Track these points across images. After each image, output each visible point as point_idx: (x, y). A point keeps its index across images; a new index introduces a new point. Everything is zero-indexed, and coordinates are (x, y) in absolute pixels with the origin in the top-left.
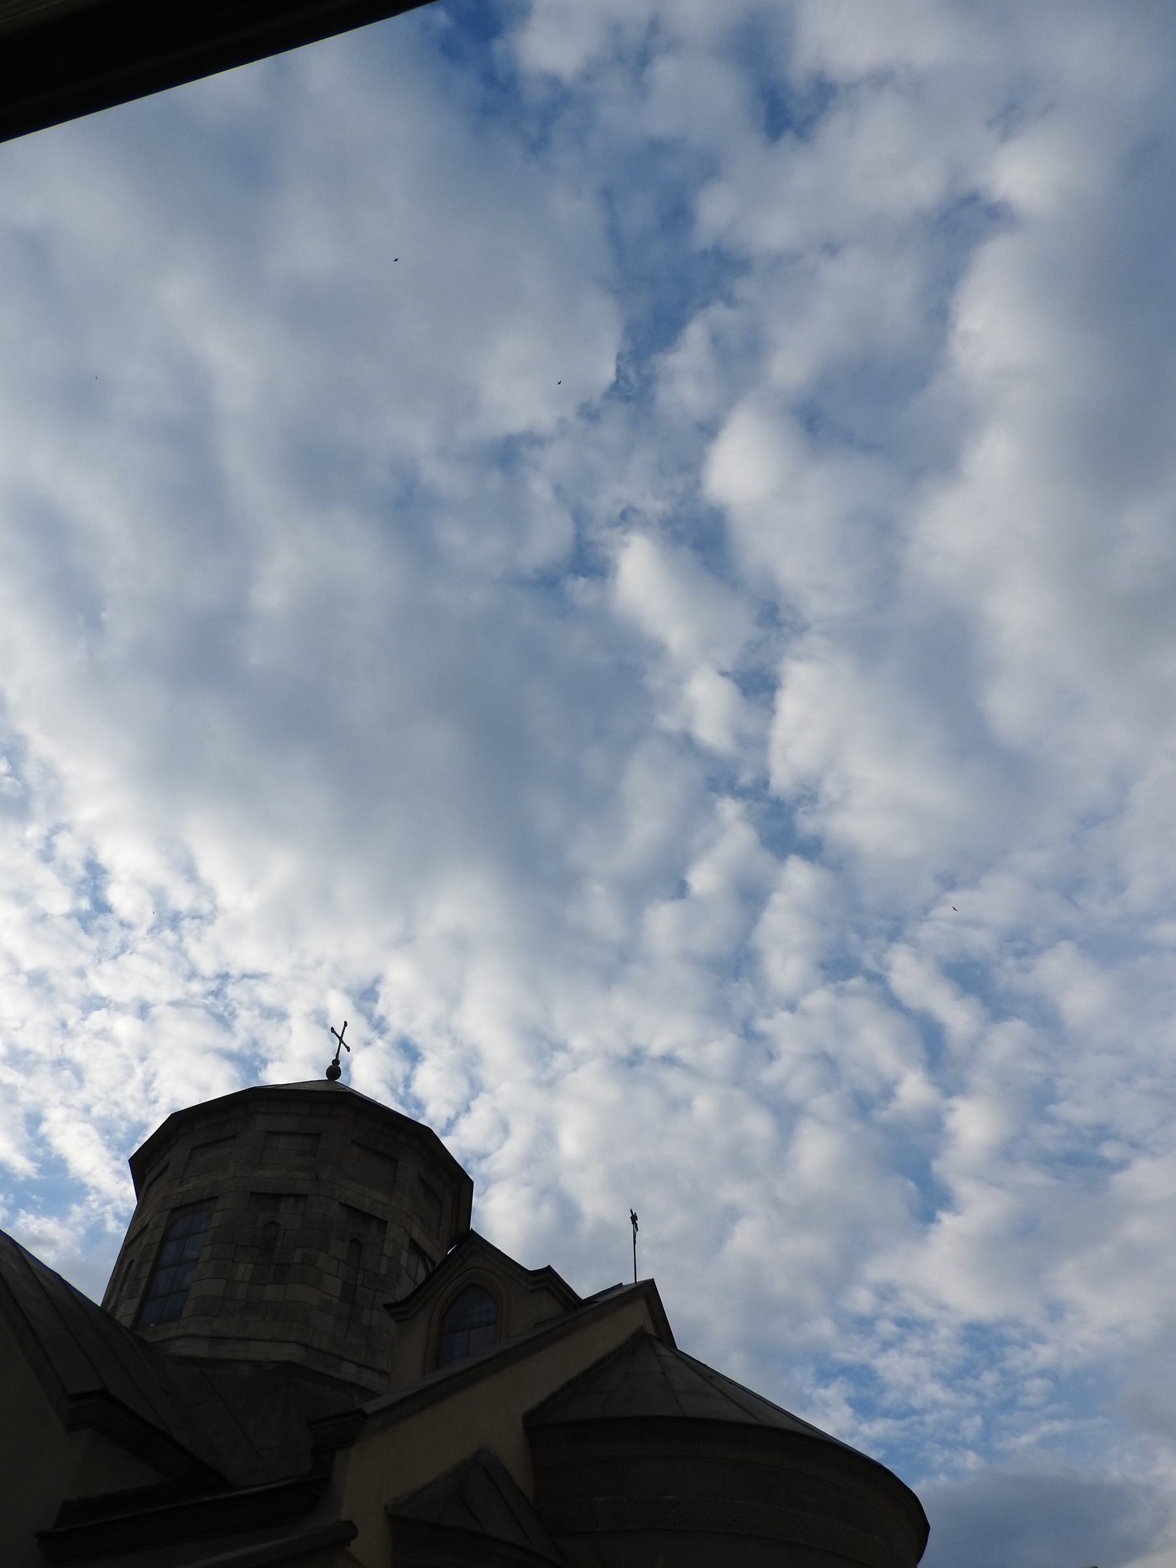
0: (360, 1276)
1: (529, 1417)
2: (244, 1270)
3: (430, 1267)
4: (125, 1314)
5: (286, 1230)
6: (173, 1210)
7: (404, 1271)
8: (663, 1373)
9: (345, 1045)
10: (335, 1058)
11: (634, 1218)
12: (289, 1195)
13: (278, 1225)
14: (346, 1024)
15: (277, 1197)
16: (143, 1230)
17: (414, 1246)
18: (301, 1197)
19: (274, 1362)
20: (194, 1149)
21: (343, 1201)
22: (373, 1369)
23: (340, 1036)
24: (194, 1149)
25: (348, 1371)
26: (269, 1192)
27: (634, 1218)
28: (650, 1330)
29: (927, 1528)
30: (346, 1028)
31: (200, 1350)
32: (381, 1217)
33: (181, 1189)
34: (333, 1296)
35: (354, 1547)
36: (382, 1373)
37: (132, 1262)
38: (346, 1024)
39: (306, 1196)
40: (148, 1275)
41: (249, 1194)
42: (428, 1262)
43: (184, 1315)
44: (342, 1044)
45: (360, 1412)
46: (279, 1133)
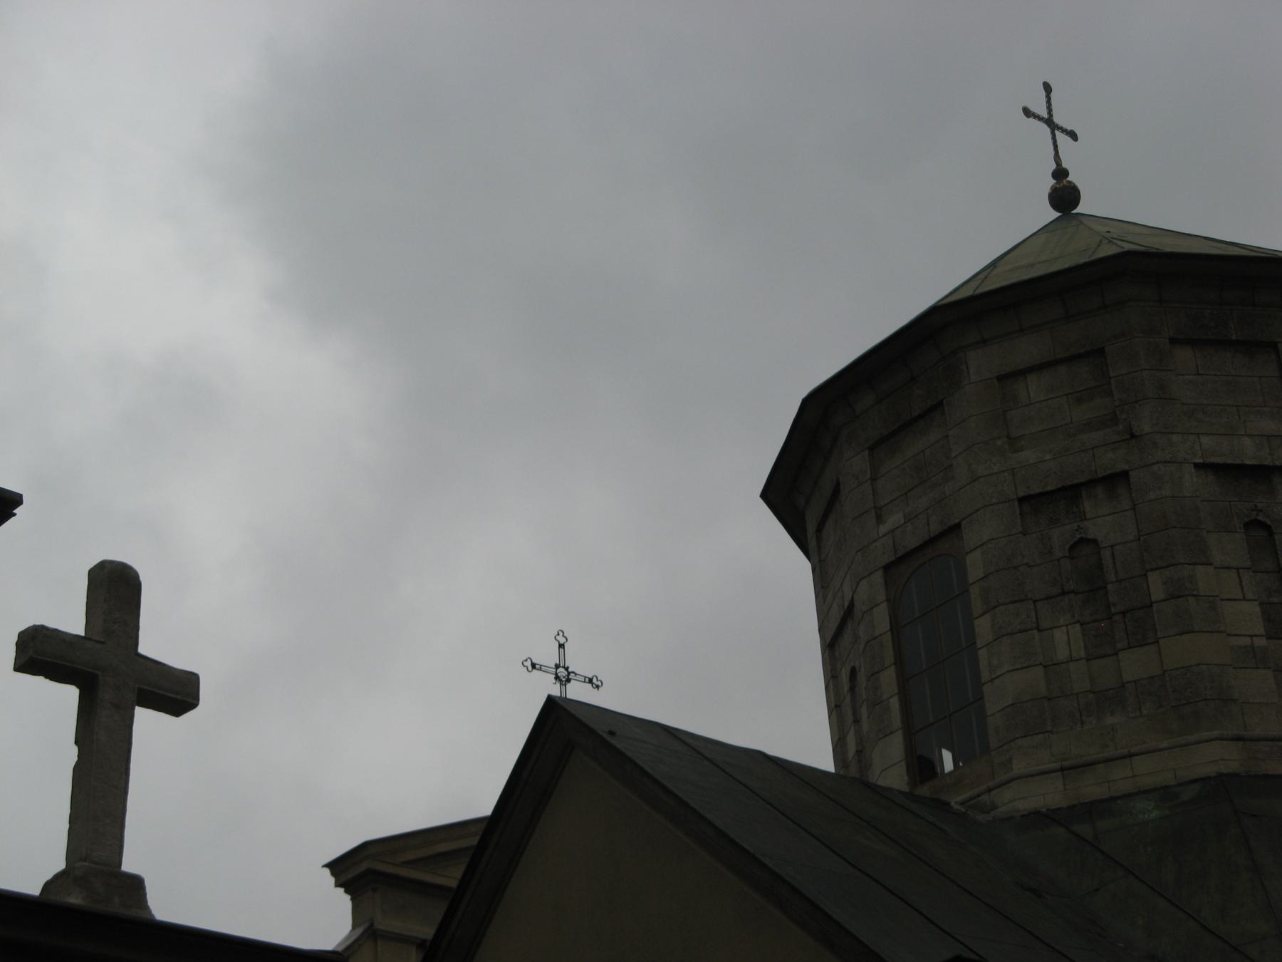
5: (1112, 547)
6: (887, 568)
9: (1064, 131)
10: (1054, 166)
12: (1092, 483)
13: (1094, 541)
14: (1047, 88)
16: (849, 613)
18: (1113, 481)
20: (871, 449)
23: (1046, 116)
26: (1049, 488)
30: (1053, 95)
31: (1050, 794)
33: (883, 529)
34: (1251, 636)
37: (853, 672)
38: (1047, 88)
39: (1125, 475)
40: (896, 690)
41: (1016, 503)
44: (1057, 132)
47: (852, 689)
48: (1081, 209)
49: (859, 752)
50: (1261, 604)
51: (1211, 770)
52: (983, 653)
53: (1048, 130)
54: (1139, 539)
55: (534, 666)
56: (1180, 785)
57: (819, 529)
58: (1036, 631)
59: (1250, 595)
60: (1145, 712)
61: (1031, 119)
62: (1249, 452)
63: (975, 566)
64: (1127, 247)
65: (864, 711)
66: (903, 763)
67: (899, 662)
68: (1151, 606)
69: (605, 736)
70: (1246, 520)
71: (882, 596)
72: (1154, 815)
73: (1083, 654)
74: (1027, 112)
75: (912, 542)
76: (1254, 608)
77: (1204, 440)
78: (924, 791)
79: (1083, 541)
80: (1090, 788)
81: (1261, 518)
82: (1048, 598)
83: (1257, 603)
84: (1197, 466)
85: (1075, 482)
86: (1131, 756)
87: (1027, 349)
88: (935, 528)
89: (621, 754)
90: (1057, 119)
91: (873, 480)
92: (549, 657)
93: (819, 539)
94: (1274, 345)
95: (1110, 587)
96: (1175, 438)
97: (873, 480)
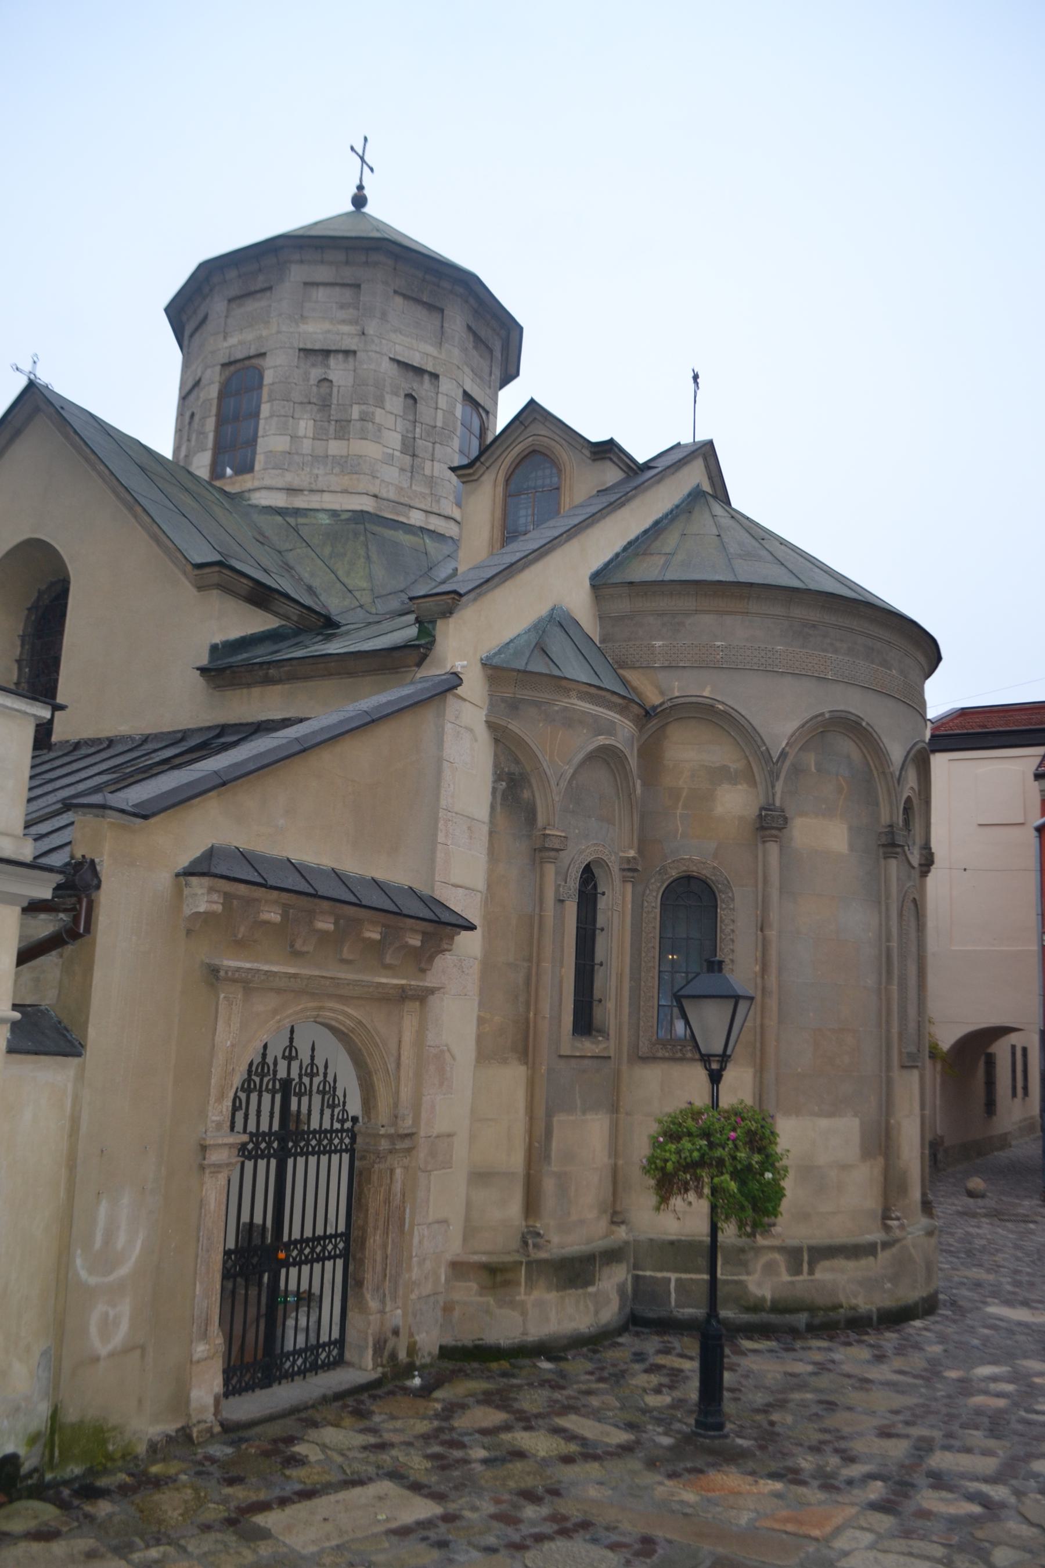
0: (418, 430)
1: (595, 576)
2: (305, 426)
3: (484, 415)
4: (201, 465)
5: (339, 386)
6: (224, 365)
7: (459, 423)
8: (719, 536)
10: (358, 182)
11: (696, 377)
12: (337, 351)
13: (331, 381)
14: (366, 139)
15: (327, 353)
16: (197, 384)
17: (467, 396)
18: (348, 353)
19: (350, 511)
20: (230, 301)
21: (392, 356)
22: (439, 515)
24: (230, 301)
25: (416, 518)
26: (317, 347)
27: (696, 377)
28: (707, 487)
29: (939, 659)
30: (368, 145)
31: (279, 500)
32: (433, 371)
33: (226, 344)
35: (460, 691)
37: (193, 415)
38: (366, 139)
39: (354, 352)
42: (481, 411)
43: (257, 467)
44: (365, 165)
45: (455, 592)
46: (316, 284)
47: (190, 423)
48: (366, 210)
49: (186, 456)
51: (358, 508)
52: (262, 422)
55: (17, 369)
56: (342, 511)
57: (191, 336)
58: (291, 419)
59: (398, 429)
62: (416, 361)
63: (269, 378)
64: (386, 236)
65: (194, 437)
66: (208, 468)
67: (218, 415)
68: (350, 421)
69: (60, 409)
70: (406, 392)
71: (217, 378)
73: (311, 435)
74: (352, 149)
75: (239, 355)
76: (399, 437)
77: (397, 346)
78: (217, 483)
79: (325, 380)
80: (300, 502)
81: (414, 394)
82: (301, 403)
84: (391, 359)
85: (330, 348)
86: (323, 491)
87: (324, 273)
88: (252, 352)
89: (65, 419)
90: (366, 158)
91: (227, 317)
92: (27, 367)
93: (190, 341)
94: (442, 311)
95: (333, 406)
96: (384, 341)
97: (227, 317)
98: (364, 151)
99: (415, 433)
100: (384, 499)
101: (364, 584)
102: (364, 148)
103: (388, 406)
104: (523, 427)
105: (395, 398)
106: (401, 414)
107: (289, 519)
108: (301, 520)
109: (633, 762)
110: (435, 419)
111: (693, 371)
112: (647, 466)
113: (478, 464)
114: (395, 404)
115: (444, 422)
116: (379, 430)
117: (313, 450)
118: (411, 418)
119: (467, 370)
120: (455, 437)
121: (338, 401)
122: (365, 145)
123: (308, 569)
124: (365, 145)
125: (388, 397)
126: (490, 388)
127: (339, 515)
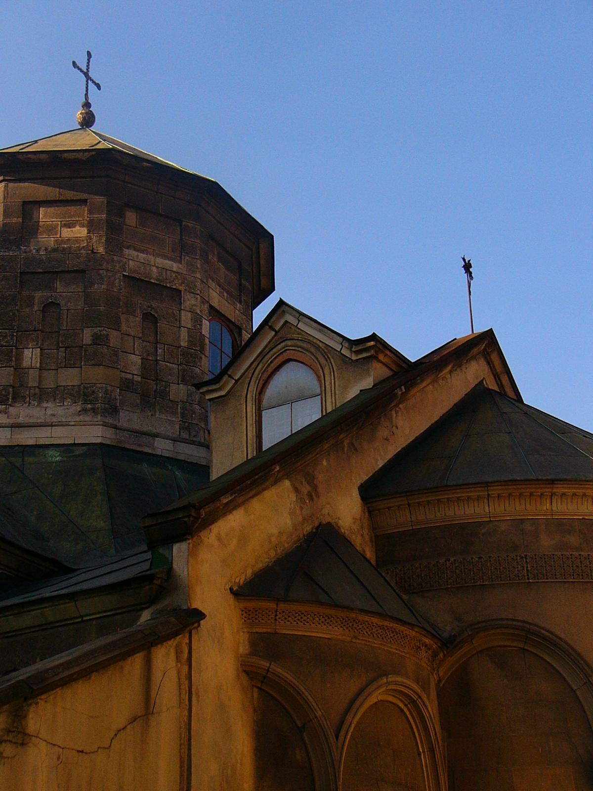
0: (160, 351)
9: (93, 82)
11: (467, 267)
13: (59, 304)
14: (89, 54)
23: (85, 71)
25: (163, 447)
27: (467, 267)
28: (492, 385)
36: (200, 444)
38: (89, 55)
39: (84, 271)
42: (230, 325)
50: (142, 359)
53: (85, 79)
54: (84, 309)
59: (137, 352)
60: (66, 404)
61: (76, 69)
70: (144, 312)
72: (58, 459)
73: (38, 365)
74: (74, 63)
76: (137, 360)
77: (130, 261)
83: (140, 357)
94: (180, 222)
98: (88, 66)
99: (156, 355)
100: (124, 430)
101: (101, 524)
102: (88, 63)
103: (124, 327)
104: (273, 333)
105: (131, 318)
106: (140, 335)
107: (13, 459)
108: (29, 460)
109: (431, 709)
110: (178, 339)
111: (464, 259)
112: (420, 362)
113: (226, 378)
114: (132, 324)
115: (189, 341)
116: (116, 354)
117: (40, 382)
118: (152, 339)
119: (213, 285)
120: (203, 357)
121: (66, 326)
122: (89, 60)
123: (35, 513)
124: (89, 60)
125: (123, 318)
126: (240, 303)
127: (73, 451)
